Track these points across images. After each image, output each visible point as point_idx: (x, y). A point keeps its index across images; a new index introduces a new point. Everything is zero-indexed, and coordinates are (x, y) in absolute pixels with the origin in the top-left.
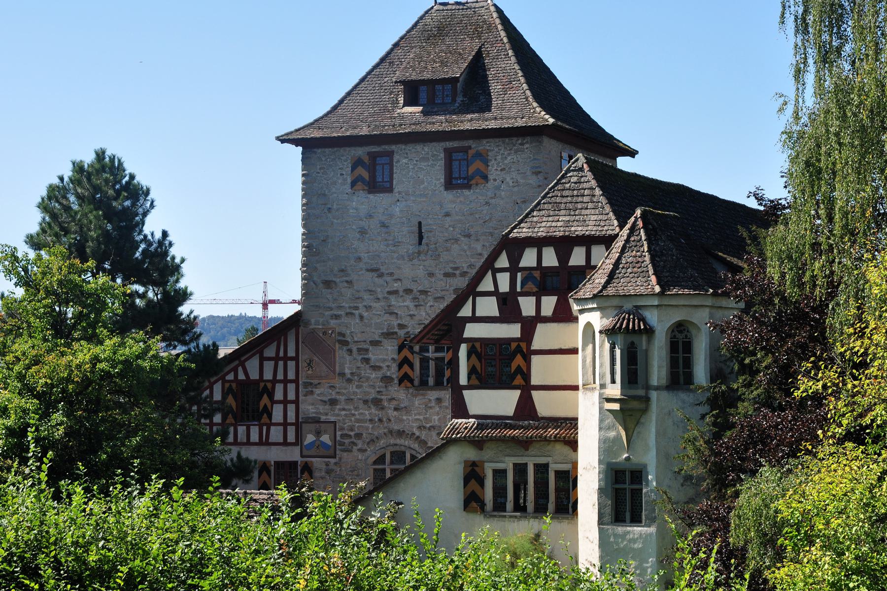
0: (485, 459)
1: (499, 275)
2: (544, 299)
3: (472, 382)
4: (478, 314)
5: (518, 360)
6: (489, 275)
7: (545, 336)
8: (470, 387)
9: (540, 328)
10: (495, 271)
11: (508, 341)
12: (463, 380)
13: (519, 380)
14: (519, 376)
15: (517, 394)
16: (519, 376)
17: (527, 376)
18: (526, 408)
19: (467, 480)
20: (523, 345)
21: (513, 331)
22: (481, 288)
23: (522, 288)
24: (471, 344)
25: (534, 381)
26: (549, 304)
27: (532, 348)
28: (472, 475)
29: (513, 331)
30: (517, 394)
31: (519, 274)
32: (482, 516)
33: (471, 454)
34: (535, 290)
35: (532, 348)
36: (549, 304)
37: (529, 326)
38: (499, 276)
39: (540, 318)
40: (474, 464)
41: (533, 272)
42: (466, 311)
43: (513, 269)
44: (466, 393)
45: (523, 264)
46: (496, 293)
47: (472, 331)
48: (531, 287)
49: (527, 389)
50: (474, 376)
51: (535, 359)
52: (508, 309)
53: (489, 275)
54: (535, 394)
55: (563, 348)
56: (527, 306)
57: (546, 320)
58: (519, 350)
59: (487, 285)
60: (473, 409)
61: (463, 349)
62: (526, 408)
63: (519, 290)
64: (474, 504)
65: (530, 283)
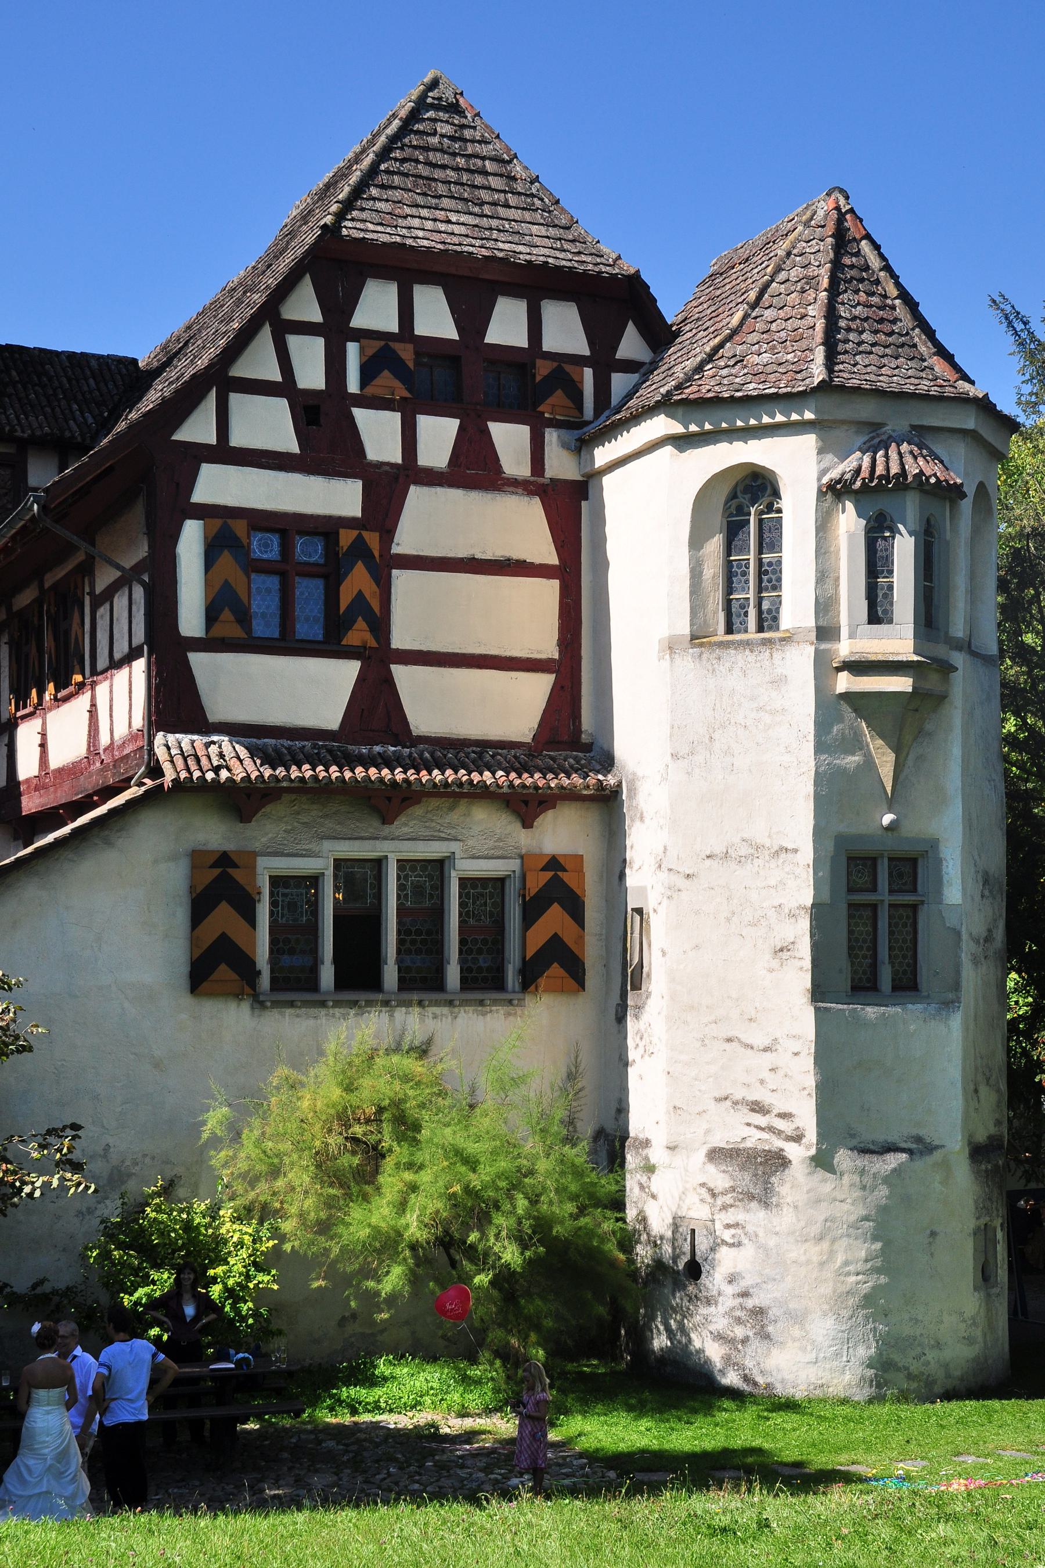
0: (257, 846)
1: (294, 342)
2: (426, 423)
3: (218, 631)
4: (238, 439)
5: (358, 581)
6: (265, 337)
7: (429, 520)
8: (209, 644)
9: (416, 496)
10: (283, 329)
11: (325, 528)
12: (191, 620)
13: (358, 634)
14: (361, 624)
15: (350, 670)
16: (361, 624)
17: (381, 625)
18: (375, 709)
19: (201, 907)
20: (372, 539)
21: (342, 498)
22: (241, 370)
23: (364, 382)
24: (218, 523)
25: (400, 639)
26: (438, 437)
27: (395, 550)
28: (217, 887)
29: (342, 498)
30: (350, 670)
31: (352, 350)
32: (245, 1006)
33: (213, 833)
34: (401, 392)
35: (395, 550)
36: (438, 437)
37: (387, 489)
38: (294, 342)
39: (410, 472)
40: (224, 860)
41: (397, 346)
42: (199, 429)
43: (336, 330)
44: (198, 660)
45: (360, 320)
46: (285, 387)
47: (217, 485)
48: (386, 382)
49: (379, 662)
50: (227, 615)
51: (402, 580)
52: (325, 437)
53: (265, 337)
54: (400, 672)
55: (479, 556)
56: (379, 434)
57: (431, 478)
58: (360, 551)
59: (260, 362)
60: (217, 710)
61: (191, 538)
62: (375, 709)
63: (353, 385)
64: (223, 971)
65: (386, 373)
